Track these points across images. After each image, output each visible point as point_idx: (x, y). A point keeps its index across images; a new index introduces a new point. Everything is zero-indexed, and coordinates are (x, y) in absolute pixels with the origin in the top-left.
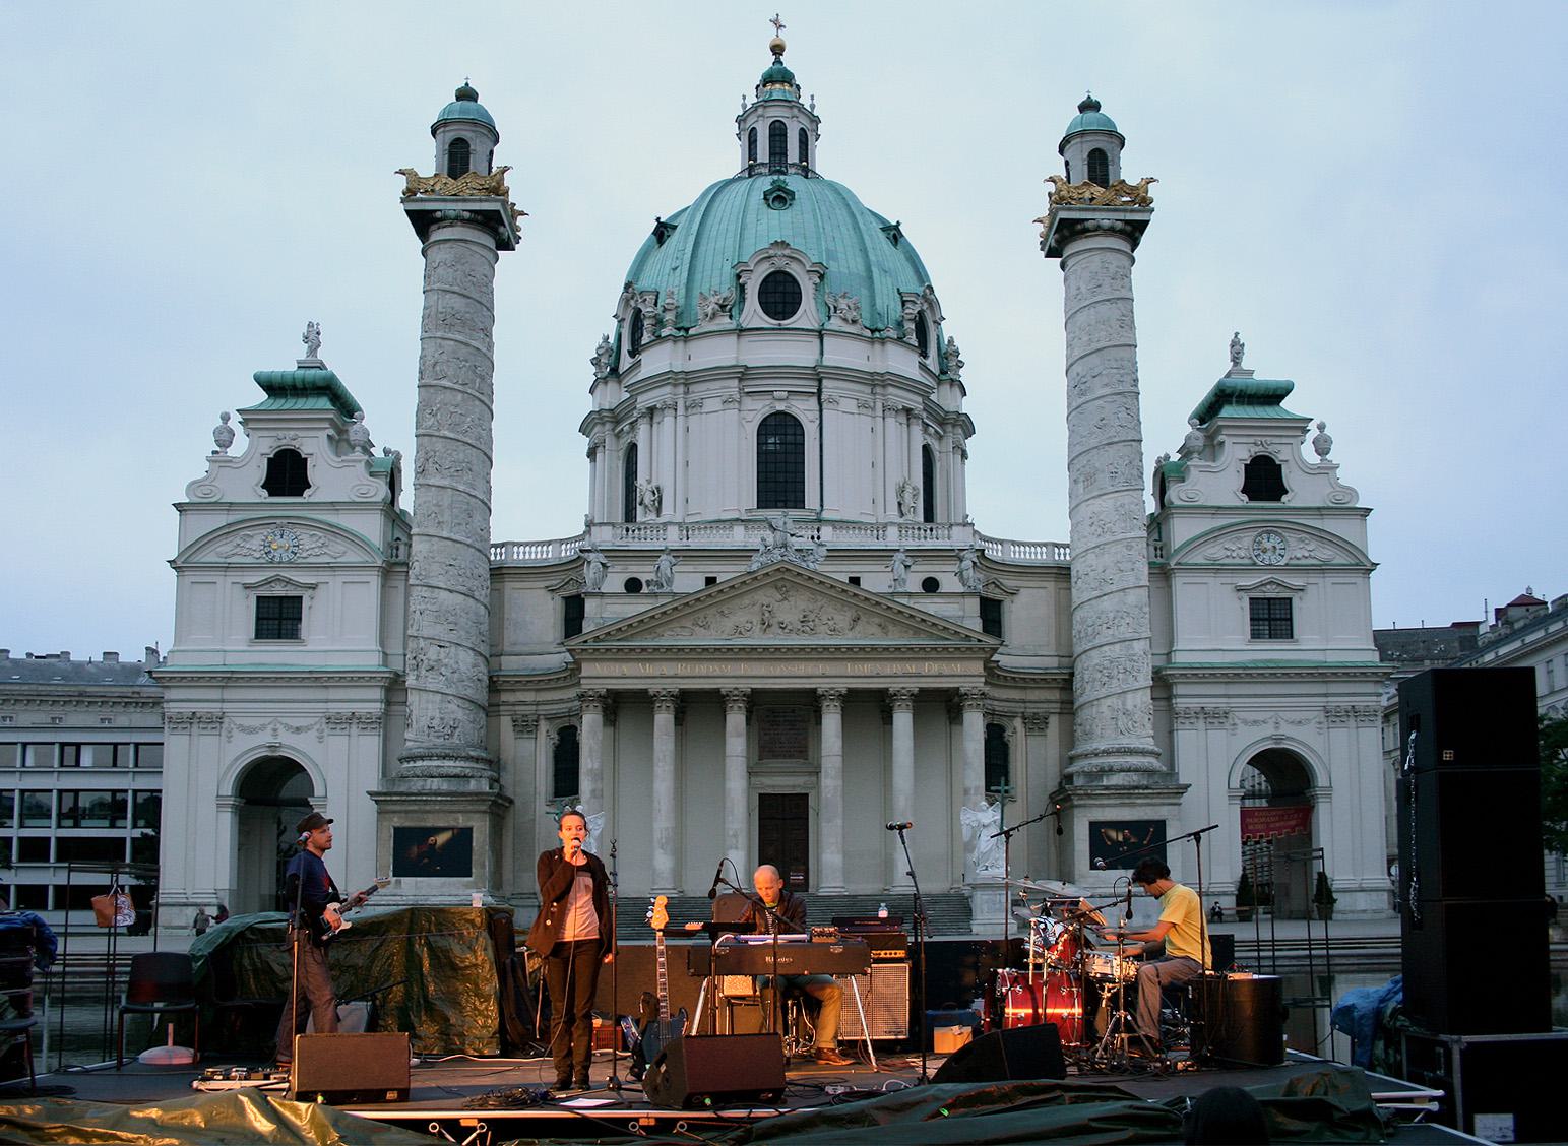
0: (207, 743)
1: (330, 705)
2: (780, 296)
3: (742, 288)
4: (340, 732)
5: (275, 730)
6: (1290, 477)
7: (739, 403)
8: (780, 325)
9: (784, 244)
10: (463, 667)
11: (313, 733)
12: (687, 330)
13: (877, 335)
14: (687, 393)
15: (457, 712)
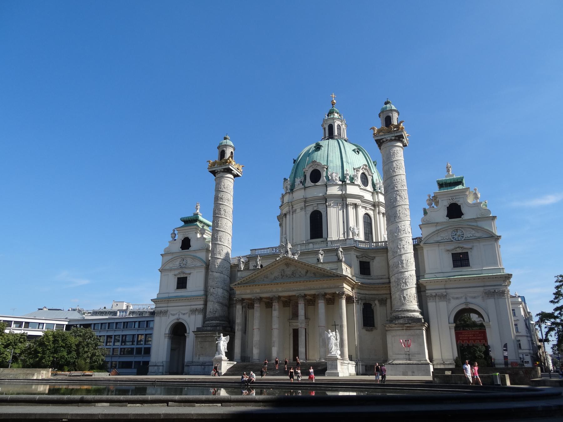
0: (164, 319)
1: (192, 307)
2: (316, 176)
3: (305, 176)
4: (193, 314)
5: (179, 314)
6: (464, 210)
7: (305, 209)
8: (315, 184)
9: (315, 161)
10: (219, 294)
11: (188, 315)
12: (293, 190)
13: (344, 183)
14: (292, 208)
15: (217, 306)
